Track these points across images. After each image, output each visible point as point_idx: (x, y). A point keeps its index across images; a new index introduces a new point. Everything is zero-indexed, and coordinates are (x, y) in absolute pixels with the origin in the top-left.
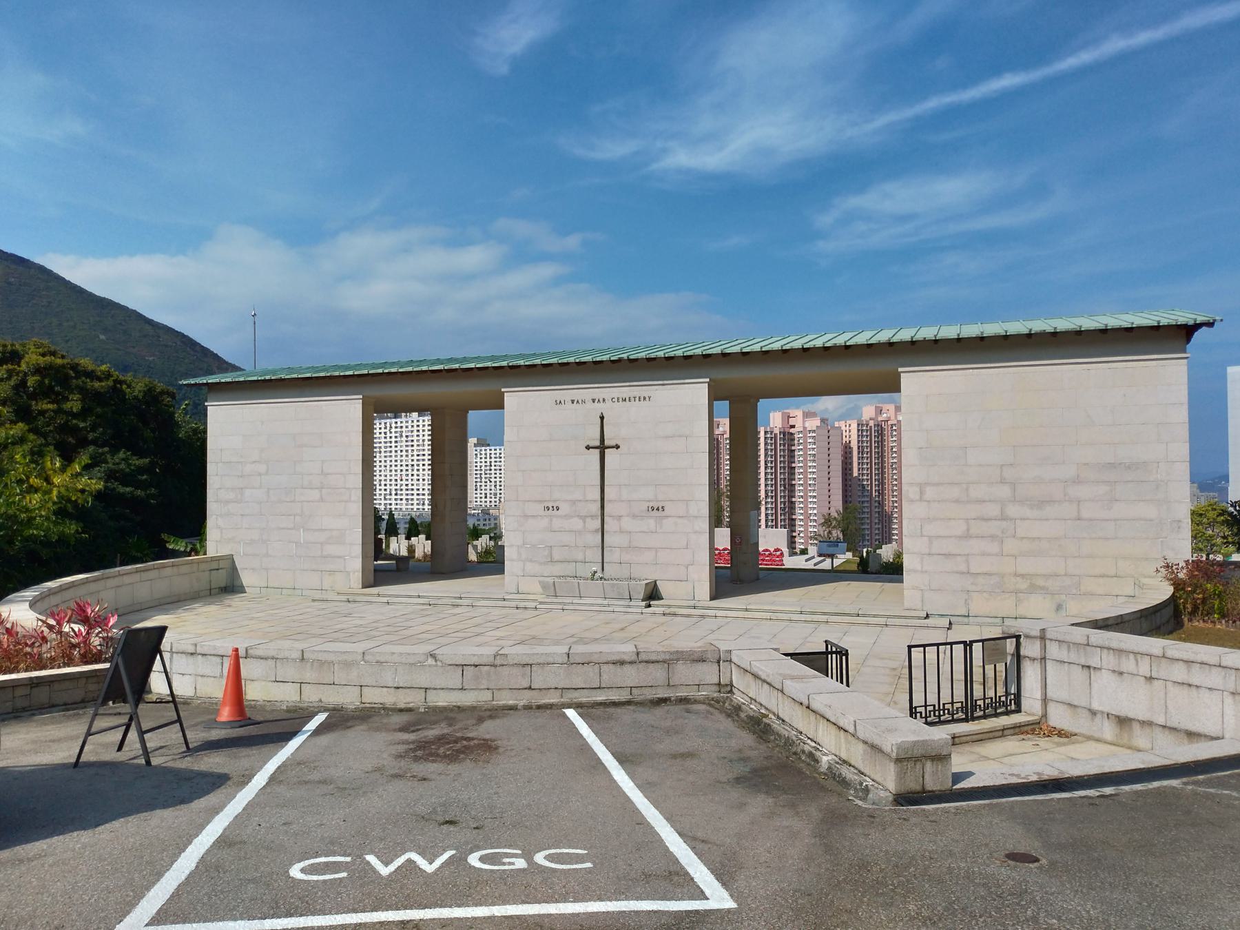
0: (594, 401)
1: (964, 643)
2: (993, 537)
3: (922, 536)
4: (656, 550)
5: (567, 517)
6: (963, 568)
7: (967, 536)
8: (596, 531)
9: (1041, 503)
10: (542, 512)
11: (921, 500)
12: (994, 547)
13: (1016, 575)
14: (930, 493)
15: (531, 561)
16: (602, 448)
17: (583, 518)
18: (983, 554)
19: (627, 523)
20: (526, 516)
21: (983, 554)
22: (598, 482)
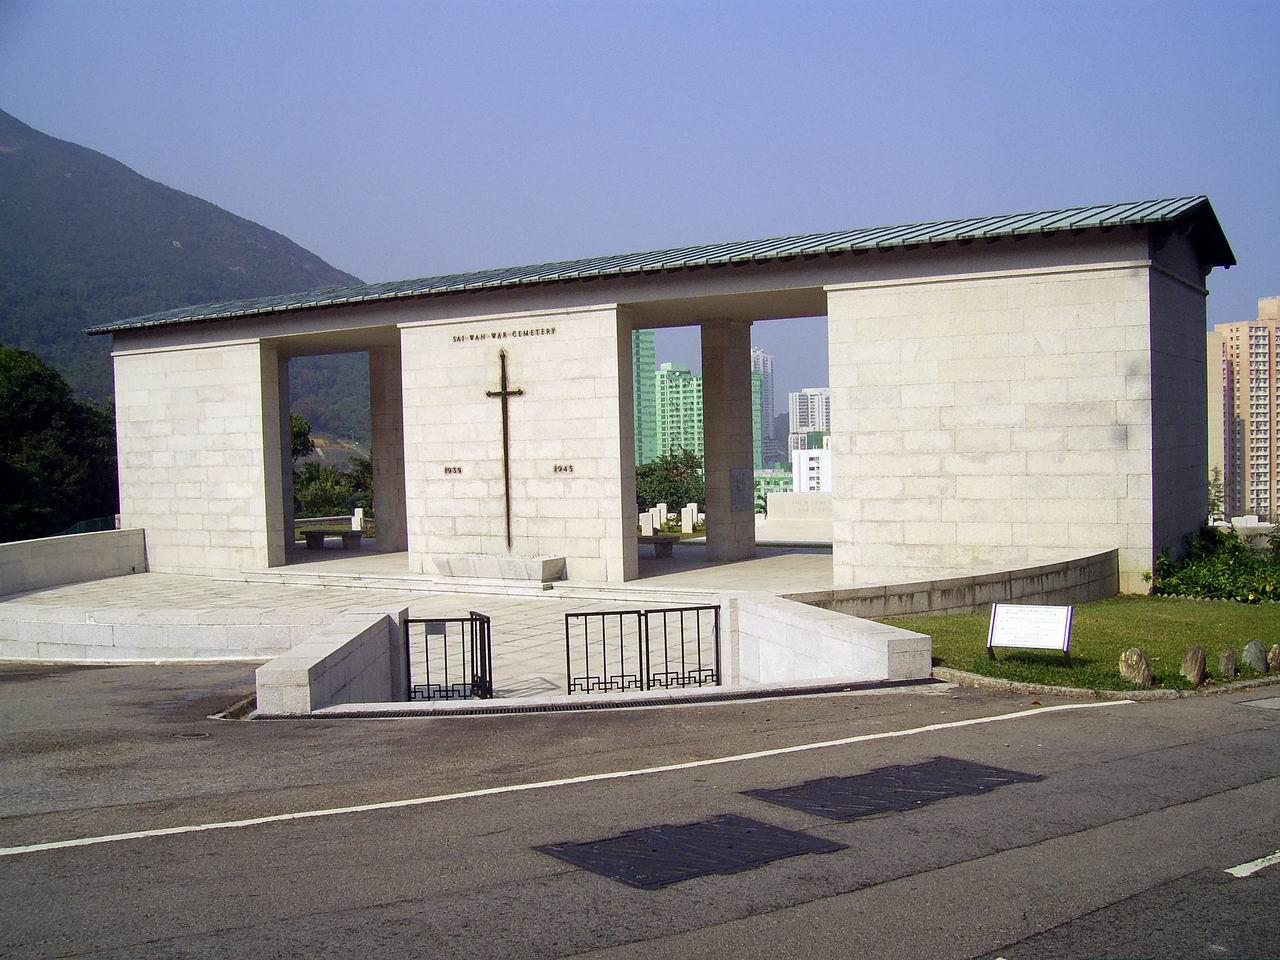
1: (638, 612)
2: (931, 499)
4: (565, 520)
5: (470, 481)
9: (983, 457)
10: (443, 475)
14: (862, 443)
16: (505, 395)
19: (535, 488)
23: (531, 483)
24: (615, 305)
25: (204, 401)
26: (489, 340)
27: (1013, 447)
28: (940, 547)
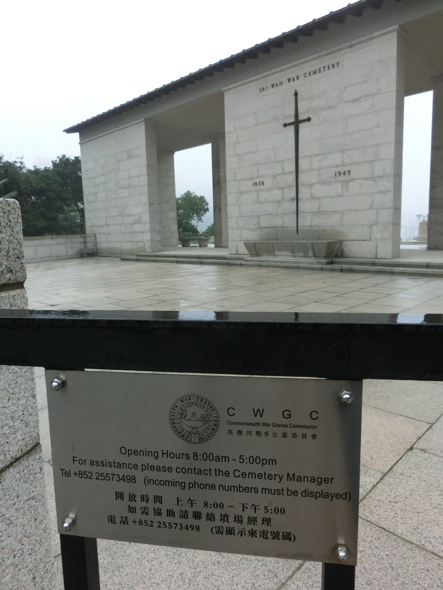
0: (289, 80)
4: (342, 212)
5: (270, 189)
8: (292, 199)
10: (252, 188)
15: (245, 229)
17: (282, 189)
19: (319, 190)
22: (293, 156)
23: (316, 186)
25: (119, 161)
26: (286, 85)
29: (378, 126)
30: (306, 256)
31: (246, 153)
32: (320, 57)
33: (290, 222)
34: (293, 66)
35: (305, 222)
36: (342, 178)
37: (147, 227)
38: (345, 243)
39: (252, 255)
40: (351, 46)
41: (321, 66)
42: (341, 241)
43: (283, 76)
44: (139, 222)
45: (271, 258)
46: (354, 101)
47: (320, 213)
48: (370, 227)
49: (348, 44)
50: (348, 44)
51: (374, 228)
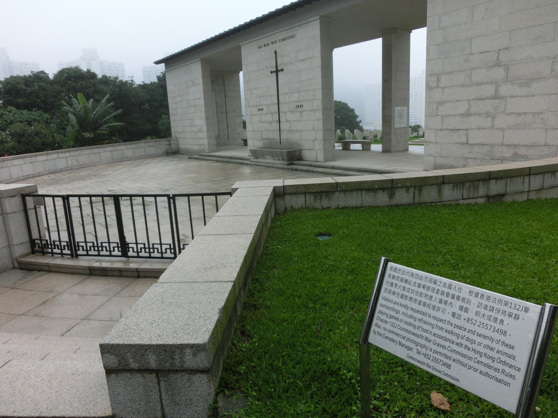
2: (487, 115)
3: (437, 115)
5: (266, 114)
6: (464, 140)
7: (467, 114)
9: (530, 81)
10: (257, 112)
11: (437, 87)
12: (487, 122)
13: (503, 145)
14: (444, 80)
17: (272, 114)
18: (479, 128)
19: (290, 116)
20: (252, 115)
21: (479, 128)
22: (276, 93)
23: (288, 114)
24: (318, 17)
27: (553, 74)
28: (493, 146)
29: (314, 78)
30: (279, 160)
31: (253, 89)
32: (286, 30)
33: (276, 136)
34: (272, 35)
35: (284, 136)
36: (299, 109)
37: (205, 135)
38: (303, 151)
39: (255, 158)
40: (300, 26)
41: (286, 36)
42: (301, 150)
43: (269, 40)
44: (200, 131)
45: (262, 160)
46: (303, 60)
47: (290, 131)
48: (313, 141)
49: (298, 24)
50: (298, 24)
51: (315, 142)
